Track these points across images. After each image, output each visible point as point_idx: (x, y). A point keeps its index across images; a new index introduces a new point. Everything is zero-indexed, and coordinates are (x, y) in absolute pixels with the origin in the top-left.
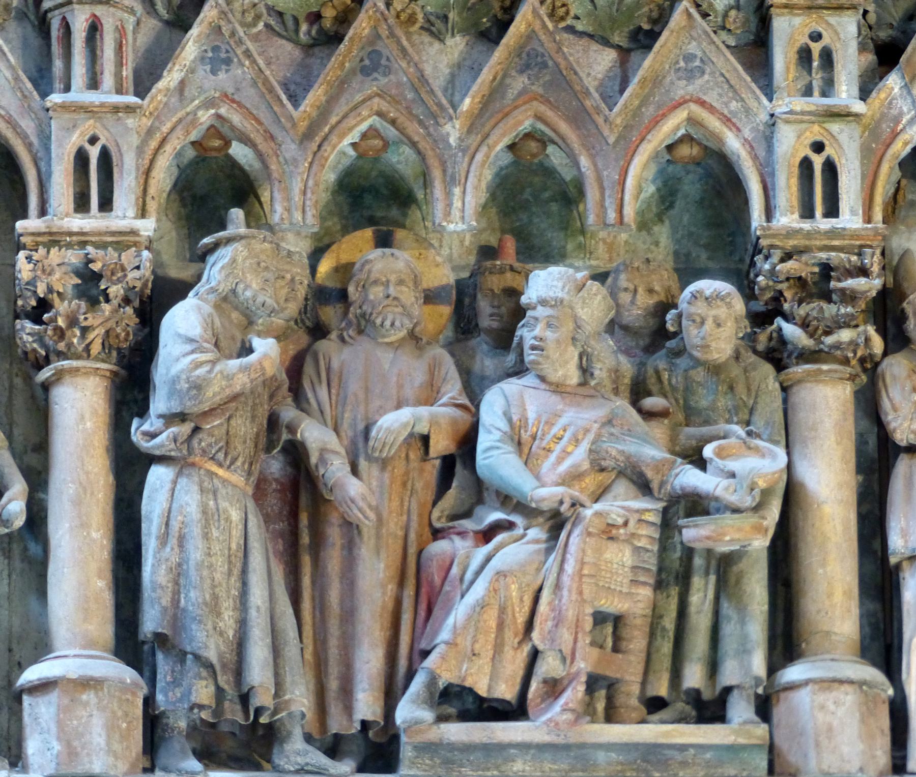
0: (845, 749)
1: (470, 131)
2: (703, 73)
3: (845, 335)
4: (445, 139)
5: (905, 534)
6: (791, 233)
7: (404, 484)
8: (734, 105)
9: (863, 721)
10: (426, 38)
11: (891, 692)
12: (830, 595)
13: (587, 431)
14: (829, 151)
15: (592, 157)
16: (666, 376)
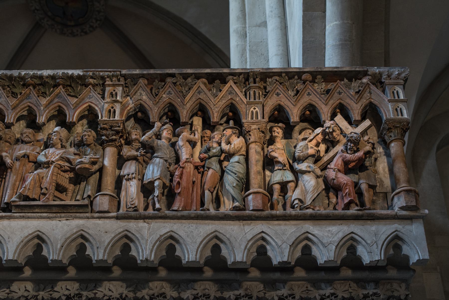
0: (105, 206)
1: (46, 107)
2: (92, 98)
3: (114, 137)
4: (41, 109)
5: (123, 172)
6: (105, 121)
7: (24, 165)
8: (97, 103)
9: (109, 202)
10: (43, 98)
11: (118, 199)
12: (107, 182)
13: (60, 153)
14: (114, 108)
15: (69, 111)
16: (81, 150)
